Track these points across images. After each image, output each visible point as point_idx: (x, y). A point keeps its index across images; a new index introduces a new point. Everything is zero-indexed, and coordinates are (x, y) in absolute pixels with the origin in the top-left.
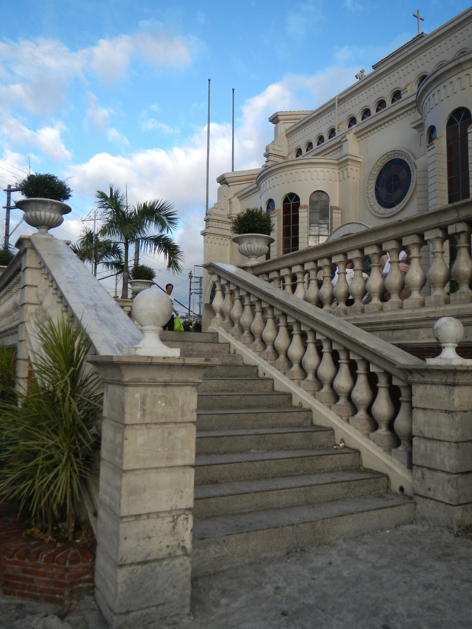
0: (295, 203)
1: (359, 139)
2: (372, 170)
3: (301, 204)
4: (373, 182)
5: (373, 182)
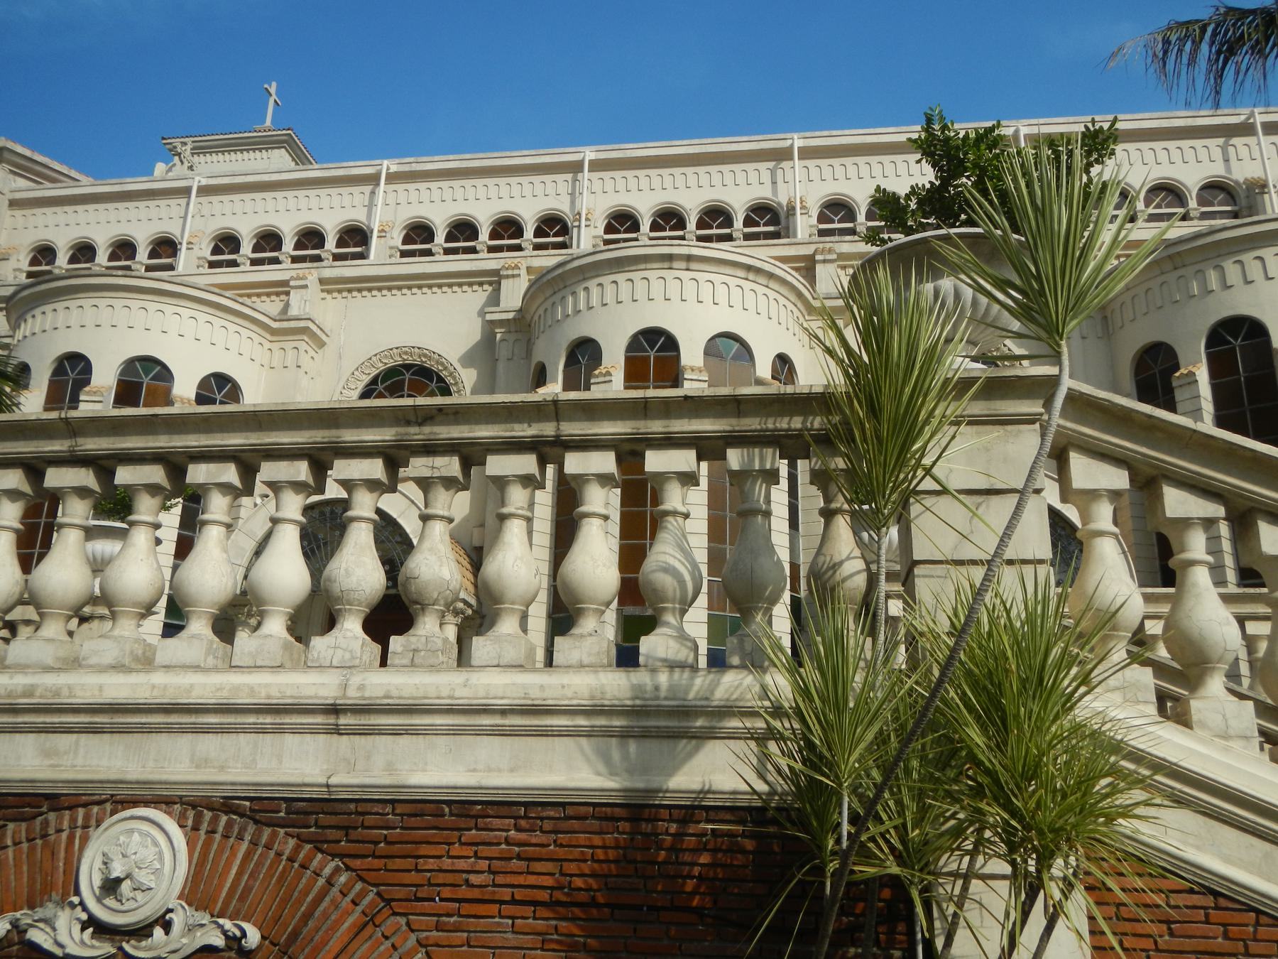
1: (325, 295)
2: (357, 369)
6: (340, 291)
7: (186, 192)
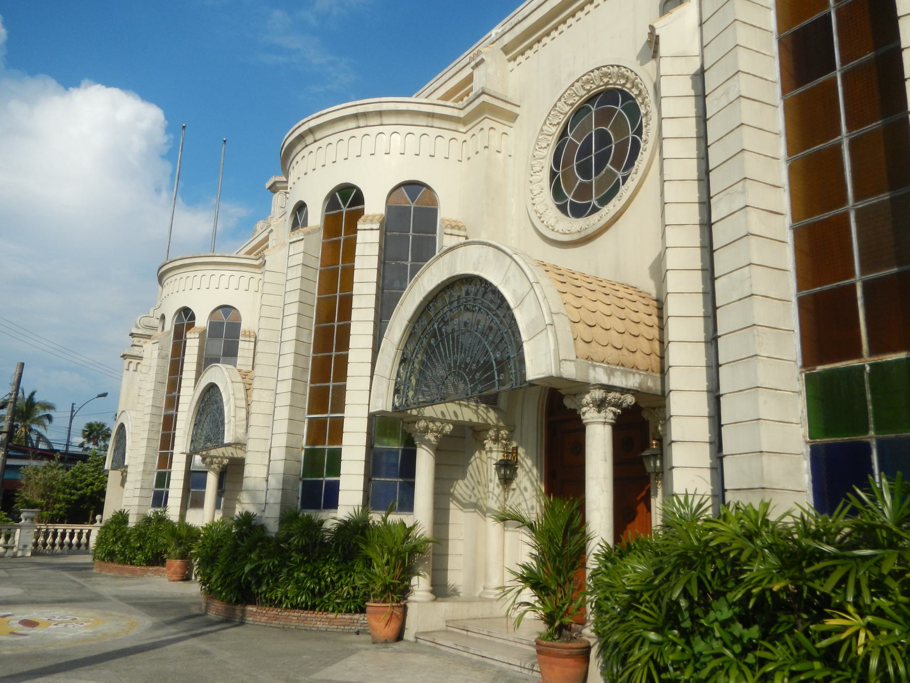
2: (545, 123)
4: (545, 154)
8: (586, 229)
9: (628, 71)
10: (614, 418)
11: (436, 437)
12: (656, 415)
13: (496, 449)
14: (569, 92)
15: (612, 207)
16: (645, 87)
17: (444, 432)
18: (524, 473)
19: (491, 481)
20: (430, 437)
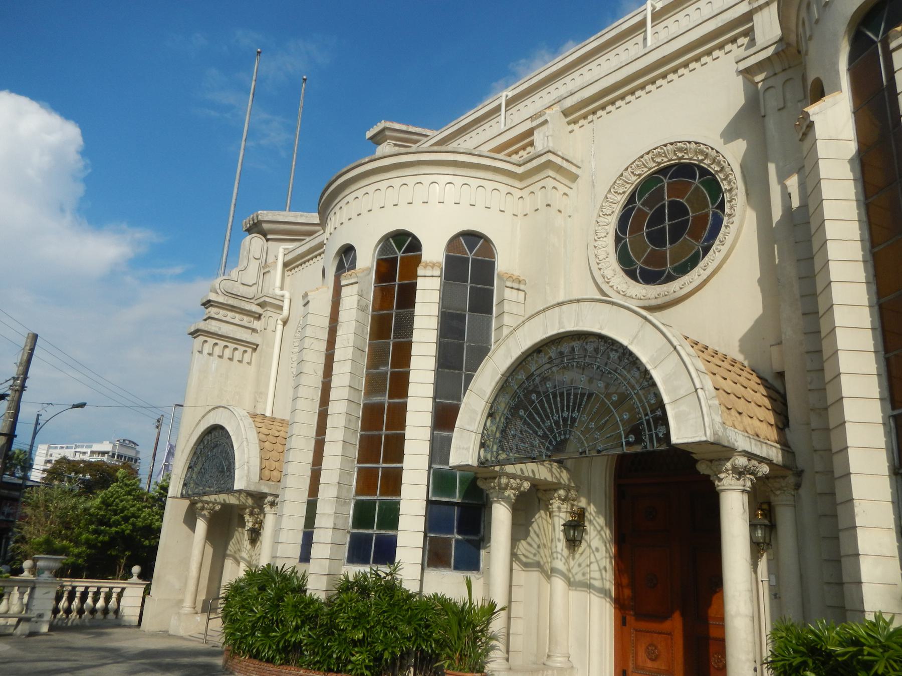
0: (408, 256)
1: (572, 126)
2: (610, 191)
3: (423, 259)
4: (610, 221)
5: (612, 223)
6: (585, 117)
7: (498, 109)
8: (665, 295)
9: (707, 148)
10: (751, 486)
11: (514, 495)
12: (769, 485)
13: (565, 510)
14: (636, 162)
15: (697, 276)
16: (729, 165)
17: (522, 489)
18: (596, 533)
19: (559, 540)
20: (510, 493)
